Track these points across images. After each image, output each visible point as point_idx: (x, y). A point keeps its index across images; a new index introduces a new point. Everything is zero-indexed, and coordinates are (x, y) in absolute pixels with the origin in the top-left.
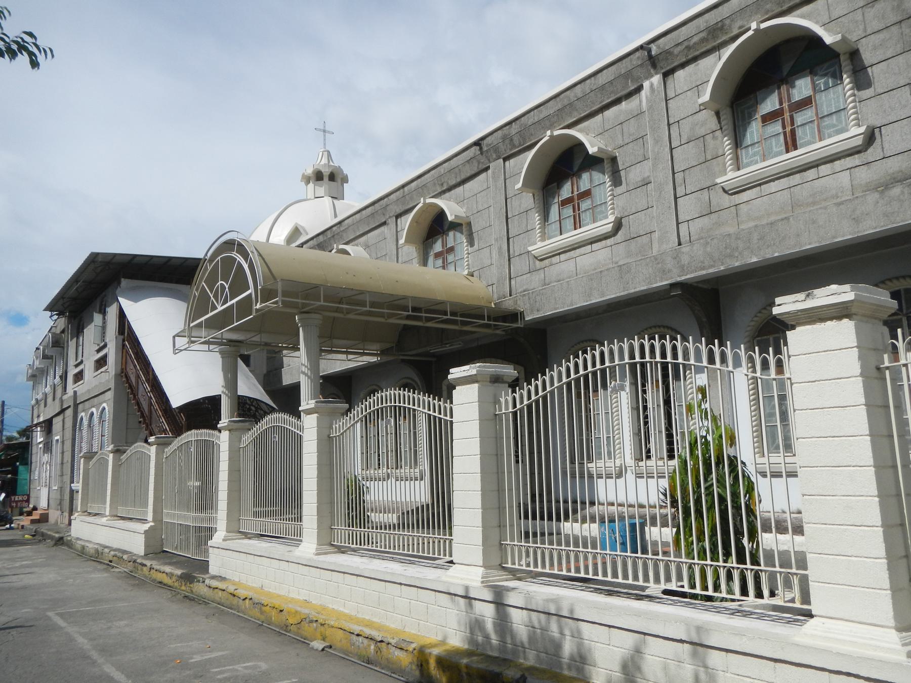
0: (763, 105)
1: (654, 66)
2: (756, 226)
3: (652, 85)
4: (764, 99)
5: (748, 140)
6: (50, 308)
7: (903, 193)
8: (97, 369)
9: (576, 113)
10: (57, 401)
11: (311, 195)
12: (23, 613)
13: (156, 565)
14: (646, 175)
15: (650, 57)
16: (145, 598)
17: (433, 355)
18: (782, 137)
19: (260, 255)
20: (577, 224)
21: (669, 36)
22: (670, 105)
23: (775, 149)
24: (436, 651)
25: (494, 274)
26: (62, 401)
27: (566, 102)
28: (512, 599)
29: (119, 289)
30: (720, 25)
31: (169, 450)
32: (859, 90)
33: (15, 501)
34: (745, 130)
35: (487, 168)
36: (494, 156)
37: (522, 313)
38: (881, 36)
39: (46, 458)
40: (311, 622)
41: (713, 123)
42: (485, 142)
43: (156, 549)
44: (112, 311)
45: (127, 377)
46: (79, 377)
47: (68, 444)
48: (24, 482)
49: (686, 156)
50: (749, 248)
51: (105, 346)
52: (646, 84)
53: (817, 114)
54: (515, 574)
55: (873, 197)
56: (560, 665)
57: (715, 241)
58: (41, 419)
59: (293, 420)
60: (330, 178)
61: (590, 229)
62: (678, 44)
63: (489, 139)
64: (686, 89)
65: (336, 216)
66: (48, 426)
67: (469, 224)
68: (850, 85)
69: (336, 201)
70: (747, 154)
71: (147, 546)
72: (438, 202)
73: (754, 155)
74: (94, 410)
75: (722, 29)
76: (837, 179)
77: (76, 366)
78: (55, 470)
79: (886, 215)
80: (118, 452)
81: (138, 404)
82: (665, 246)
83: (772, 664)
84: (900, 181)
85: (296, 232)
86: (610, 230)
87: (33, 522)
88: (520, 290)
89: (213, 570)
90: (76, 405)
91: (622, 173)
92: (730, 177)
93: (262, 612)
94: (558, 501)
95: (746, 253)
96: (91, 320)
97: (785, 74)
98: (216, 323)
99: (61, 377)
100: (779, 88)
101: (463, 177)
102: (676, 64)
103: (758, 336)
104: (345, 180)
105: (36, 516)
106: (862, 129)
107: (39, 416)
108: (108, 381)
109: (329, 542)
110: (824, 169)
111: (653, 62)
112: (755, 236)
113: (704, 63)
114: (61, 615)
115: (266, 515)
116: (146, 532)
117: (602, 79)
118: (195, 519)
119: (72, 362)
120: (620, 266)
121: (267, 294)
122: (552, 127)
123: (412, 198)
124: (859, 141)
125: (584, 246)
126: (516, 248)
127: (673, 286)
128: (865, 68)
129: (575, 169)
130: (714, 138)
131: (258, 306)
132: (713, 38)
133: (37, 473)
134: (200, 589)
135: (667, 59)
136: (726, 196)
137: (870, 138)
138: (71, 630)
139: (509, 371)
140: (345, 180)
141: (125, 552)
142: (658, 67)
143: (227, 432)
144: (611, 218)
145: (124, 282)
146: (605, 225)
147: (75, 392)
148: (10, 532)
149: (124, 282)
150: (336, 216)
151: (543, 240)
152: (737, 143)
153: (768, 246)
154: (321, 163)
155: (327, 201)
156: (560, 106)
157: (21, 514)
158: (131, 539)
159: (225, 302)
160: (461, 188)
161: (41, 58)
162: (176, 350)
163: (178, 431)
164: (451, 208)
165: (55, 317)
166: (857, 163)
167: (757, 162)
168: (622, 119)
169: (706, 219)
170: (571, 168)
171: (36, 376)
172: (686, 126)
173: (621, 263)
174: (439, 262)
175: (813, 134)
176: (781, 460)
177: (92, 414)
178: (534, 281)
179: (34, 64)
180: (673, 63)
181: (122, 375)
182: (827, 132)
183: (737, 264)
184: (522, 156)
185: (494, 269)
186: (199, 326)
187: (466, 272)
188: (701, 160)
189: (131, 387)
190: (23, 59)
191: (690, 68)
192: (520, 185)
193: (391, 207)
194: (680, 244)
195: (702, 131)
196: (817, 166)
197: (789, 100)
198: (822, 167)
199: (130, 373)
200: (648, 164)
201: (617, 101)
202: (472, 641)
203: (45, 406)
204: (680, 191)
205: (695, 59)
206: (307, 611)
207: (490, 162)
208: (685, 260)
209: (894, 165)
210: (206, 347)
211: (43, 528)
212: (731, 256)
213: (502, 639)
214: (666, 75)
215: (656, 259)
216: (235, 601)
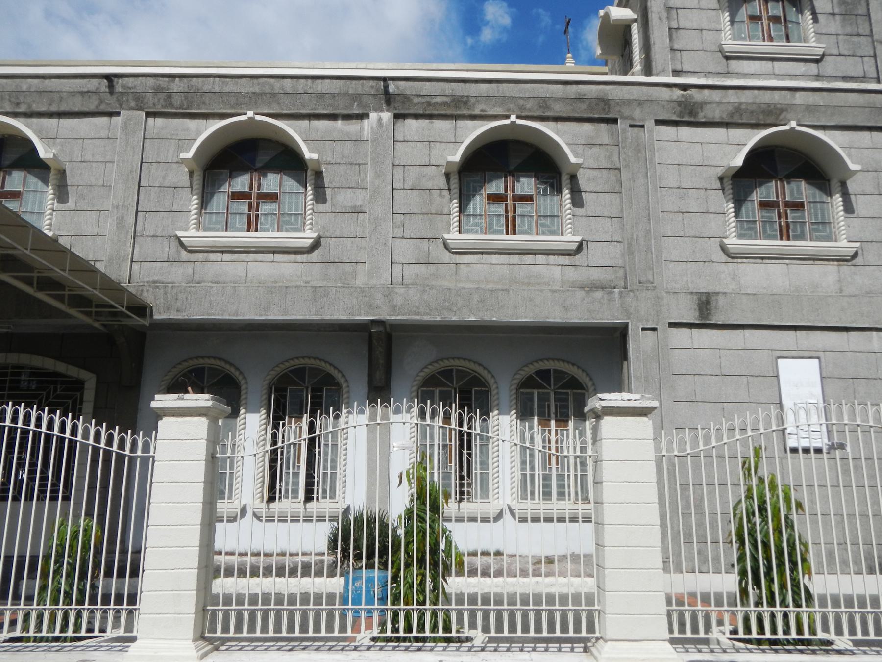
3: (380, 119)
4: (490, 181)
5: (471, 210)
7: (603, 297)
14: (359, 203)
22: (397, 147)
27: (267, 89)
30: (465, 99)
35: (118, 114)
42: (120, 81)
50: (468, 306)
52: (373, 116)
55: (580, 294)
57: (434, 291)
61: (267, 236)
62: (420, 95)
63: (130, 82)
64: (416, 138)
73: (476, 224)
75: (466, 103)
76: (553, 271)
79: (589, 311)
82: (374, 282)
84: (603, 288)
86: (307, 245)
88: (147, 279)
91: (328, 191)
94: (124, 552)
95: (464, 310)
97: (512, 168)
100: (506, 177)
101: (64, 108)
102: (411, 111)
103: (422, 387)
110: (541, 259)
111: (388, 99)
112: (476, 297)
120: (316, 287)
124: (574, 246)
125: (263, 252)
135: (403, 103)
136: (447, 252)
137: (580, 248)
142: (392, 105)
146: (306, 237)
153: (487, 310)
156: (257, 89)
160: (54, 121)
166: (568, 263)
167: (476, 232)
168: (335, 136)
173: (314, 284)
175: (530, 226)
178: (177, 274)
180: (409, 109)
183: (454, 318)
188: (424, 211)
191: (424, 122)
195: (429, 185)
196: (535, 254)
201: (333, 117)
205: (430, 117)
209: (596, 274)
212: (449, 309)
214: (397, 116)
215: (363, 292)
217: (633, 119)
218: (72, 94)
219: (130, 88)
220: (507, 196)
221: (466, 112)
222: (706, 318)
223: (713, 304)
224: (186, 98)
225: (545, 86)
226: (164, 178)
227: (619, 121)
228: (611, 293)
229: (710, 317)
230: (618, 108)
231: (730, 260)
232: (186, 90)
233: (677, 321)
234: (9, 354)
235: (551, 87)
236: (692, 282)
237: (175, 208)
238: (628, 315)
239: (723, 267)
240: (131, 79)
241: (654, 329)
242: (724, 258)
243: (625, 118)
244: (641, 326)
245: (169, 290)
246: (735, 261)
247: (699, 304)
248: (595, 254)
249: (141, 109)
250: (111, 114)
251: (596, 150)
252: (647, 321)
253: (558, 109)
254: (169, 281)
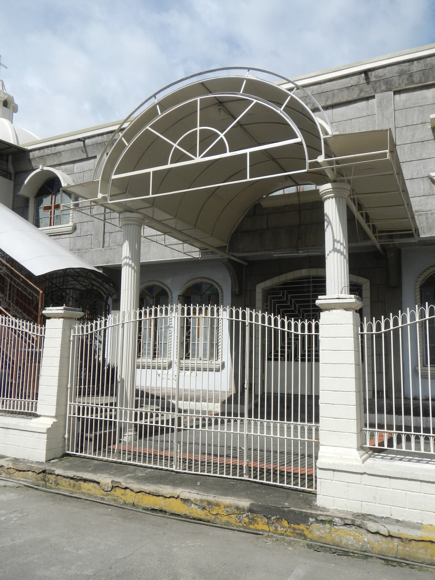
35: (373, 97)
36: (384, 88)
42: (373, 73)
71: (49, 449)
101: (336, 101)
104: (15, 109)
140: (15, 109)
207: (375, 91)
218: (341, 90)
219: (381, 77)
224: (424, 74)
226: (413, 136)
232: (424, 68)
234: (311, 269)
237: (424, 156)
240: (381, 70)
245: (429, 215)
249: (389, 90)
250: (367, 99)
254: (427, 209)
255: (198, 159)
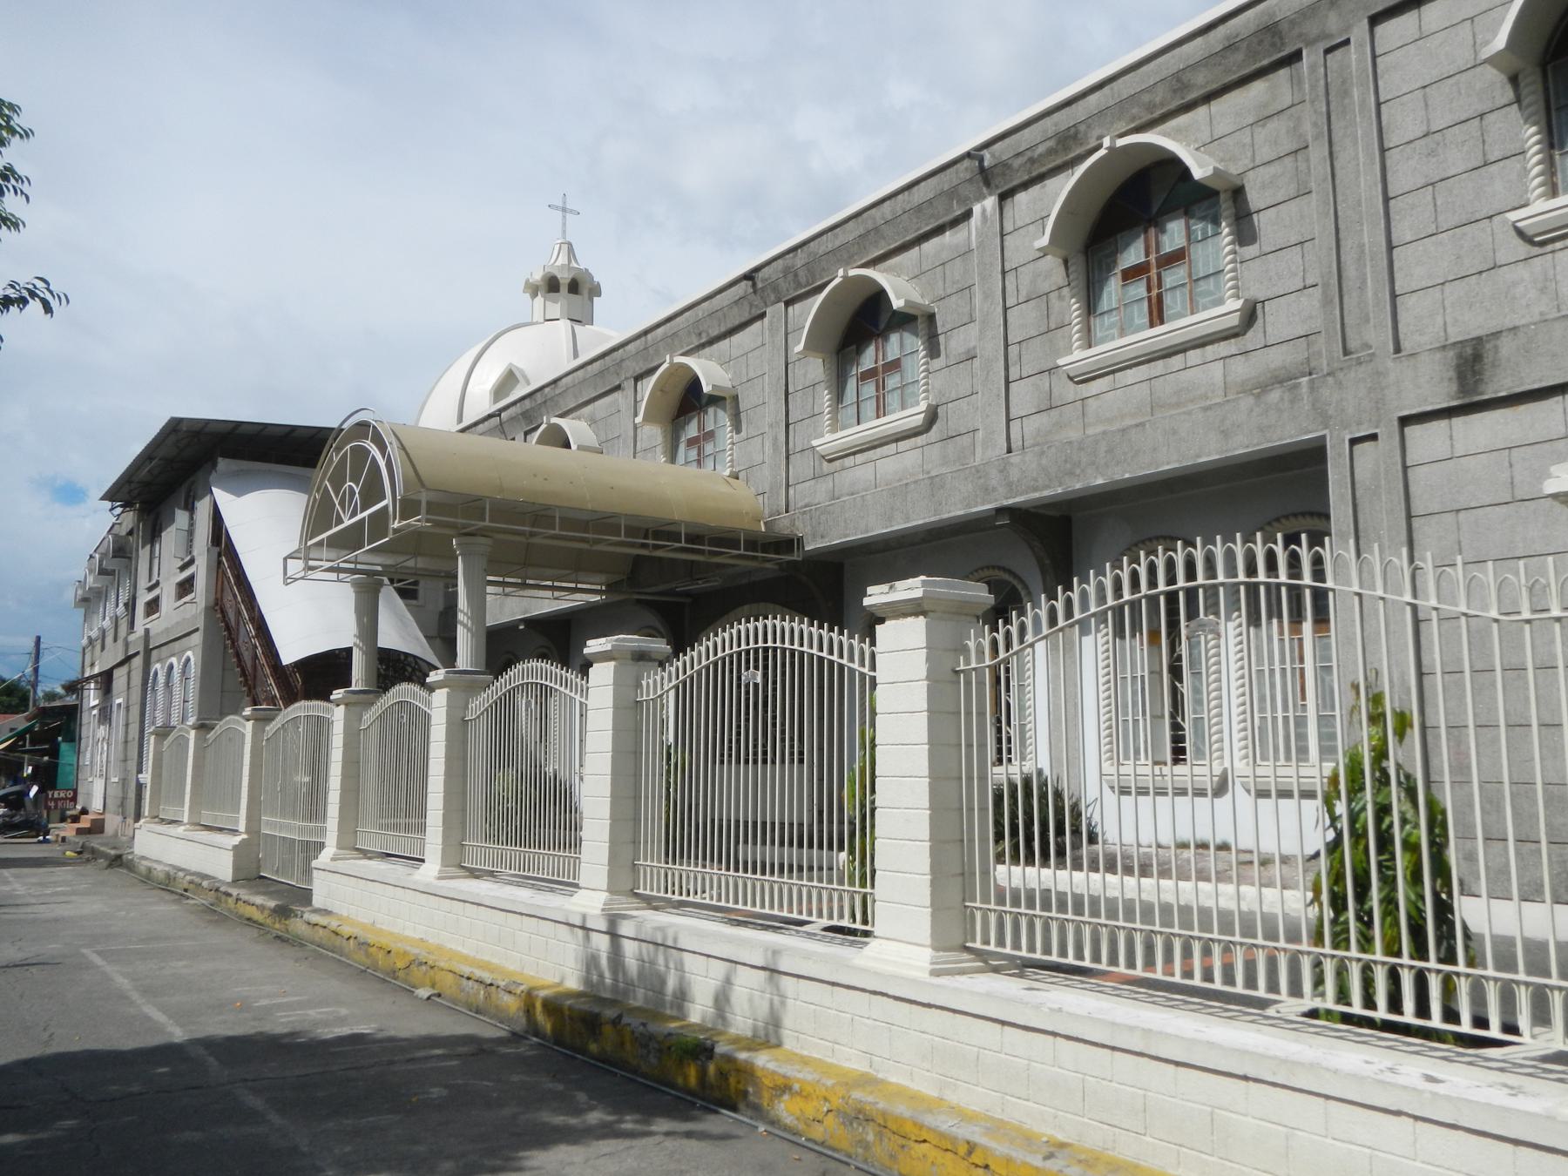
0: (1125, 255)
1: (987, 183)
2: (1104, 433)
3: (984, 211)
4: (1127, 245)
6: (110, 496)
7: (1282, 399)
8: (180, 596)
9: (883, 243)
10: (120, 641)
11: (538, 317)
12: (52, 948)
13: (244, 894)
14: (972, 344)
15: (982, 169)
16: (219, 937)
17: (687, 594)
18: (1146, 304)
19: (403, 448)
20: (881, 411)
21: (1007, 141)
23: (1137, 321)
24: (543, 993)
25: (768, 475)
26: (127, 645)
27: (870, 226)
28: (626, 928)
29: (214, 475)
31: (271, 728)
32: (1241, 245)
33: (56, 800)
34: (1101, 290)
35: (763, 315)
36: (773, 298)
37: (800, 540)
38: (1272, 169)
39: (102, 731)
40: (421, 964)
41: (1059, 276)
42: (761, 275)
43: (249, 874)
44: (203, 508)
45: (223, 611)
46: (153, 606)
47: (135, 711)
48: (68, 769)
49: (1024, 320)
51: (192, 562)
52: (977, 209)
53: (1190, 275)
54: (650, 903)
56: (662, 1003)
57: (1053, 450)
58: (96, 670)
59: (424, 693)
60: (570, 289)
62: (1018, 155)
65: (576, 355)
66: (106, 680)
67: (736, 398)
68: (1229, 238)
69: (578, 328)
70: (1102, 325)
72: (690, 361)
73: (1111, 327)
74: (174, 660)
75: (1075, 137)
77: (150, 589)
78: (116, 751)
79: (1261, 429)
80: (203, 727)
81: (238, 655)
83: (829, 987)
84: (1281, 382)
85: (510, 378)
87: (80, 832)
89: (317, 901)
90: (148, 652)
91: (942, 338)
92: (1077, 357)
93: (368, 955)
96: (173, 521)
97: (1155, 210)
98: (349, 540)
99: (126, 605)
100: (1146, 232)
101: (730, 325)
102: (1015, 182)
104: (596, 291)
105: (85, 822)
106: (1238, 304)
107: (92, 665)
108: (195, 617)
109: (458, 863)
110: (1194, 356)
111: (986, 177)
112: (1103, 447)
113: (1051, 183)
114: (99, 953)
115: (388, 827)
116: (235, 847)
117: (920, 195)
118: (301, 830)
119: (143, 583)
121: (408, 507)
122: (847, 263)
123: (657, 352)
124: (1234, 320)
126: (797, 442)
127: (1000, 511)
128: (1250, 214)
129: (882, 326)
130: (1061, 298)
131: (396, 525)
132: (1066, 147)
133: (88, 755)
134: (297, 926)
137: (1250, 315)
138: (109, 969)
139: (660, 646)
140: (596, 291)
141: (205, 877)
143: (342, 707)
144: (923, 406)
145: (223, 464)
146: (913, 416)
147: (147, 631)
148: (44, 846)
149: (223, 464)
150: (576, 355)
151: (834, 430)
152: (1091, 306)
153: (1118, 463)
154: (557, 263)
155: (564, 326)
157: (63, 819)
158: (214, 858)
159: (354, 514)
160: (727, 341)
161: (54, 303)
162: (288, 580)
163: (290, 698)
164: (710, 372)
165: (119, 510)
167: (1113, 339)
168: (945, 256)
169: (1044, 418)
170: (876, 326)
171: (89, 601)
172: (1026, 275)
173: (933, 474)
174: (693, 454)
176: (1269, 771)
177: (171, 667)
178: (818, 493)
179: (48, 308)
181: (216, 608)
182: (1202, 301)
184: (810, 300)
185: (766, 470)
186: (320, 544)
187: (727, 472)
189: (228, 628)
190: (35, 306)
191: (1035, 190)
192: (800, 347)
193: (627, 363)
194: (1009, 451)
195: (1045, 286)
196: (1184, 351)
197: (1158, 251)
198: (1191, 353)
199: (228, 605)
200: (974, 329)
201: (939, 230)
202: (587, 981)
203: (103, 648)
204: (1014, 375)
205: (1041, 178)
206: (416, 951)
208: (1014, 474)
209: (1277, 358)
210: (333, 576)
211: (95, 842)
212: (1071, 473)
213: (615, 980)
214: (1004, 197)
216: (338, 941)
217: (1330, 36)
220: (1148, 263)
221: (1079, 151)
222: (1475, 392)
223: (1488, 358)
225: (1177, 51)
226: (805, 376)
227: (1304, 53)
228: (1297, 386)
229: (1482, 387)
230: (1296, 31)
231: (1537, 250)
233: (1414, 411)
235: (1186, 48)
236: (1456, 321)
238: (1325, 420)
239: (1522, 271)
241: (1373, 437)
242: (1523, 249)
243: (1311, 43)
244: (1348, 437)
246: (1549, 248)
247: (1458, 366)
248: (1279, 321)
251: (1272, 125)
252: (1359, 423)
253: (1203, 81)
255: (347, 523)
